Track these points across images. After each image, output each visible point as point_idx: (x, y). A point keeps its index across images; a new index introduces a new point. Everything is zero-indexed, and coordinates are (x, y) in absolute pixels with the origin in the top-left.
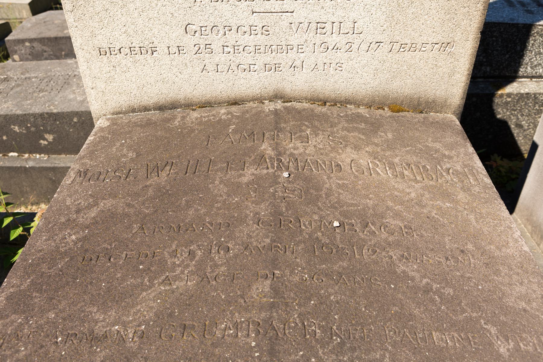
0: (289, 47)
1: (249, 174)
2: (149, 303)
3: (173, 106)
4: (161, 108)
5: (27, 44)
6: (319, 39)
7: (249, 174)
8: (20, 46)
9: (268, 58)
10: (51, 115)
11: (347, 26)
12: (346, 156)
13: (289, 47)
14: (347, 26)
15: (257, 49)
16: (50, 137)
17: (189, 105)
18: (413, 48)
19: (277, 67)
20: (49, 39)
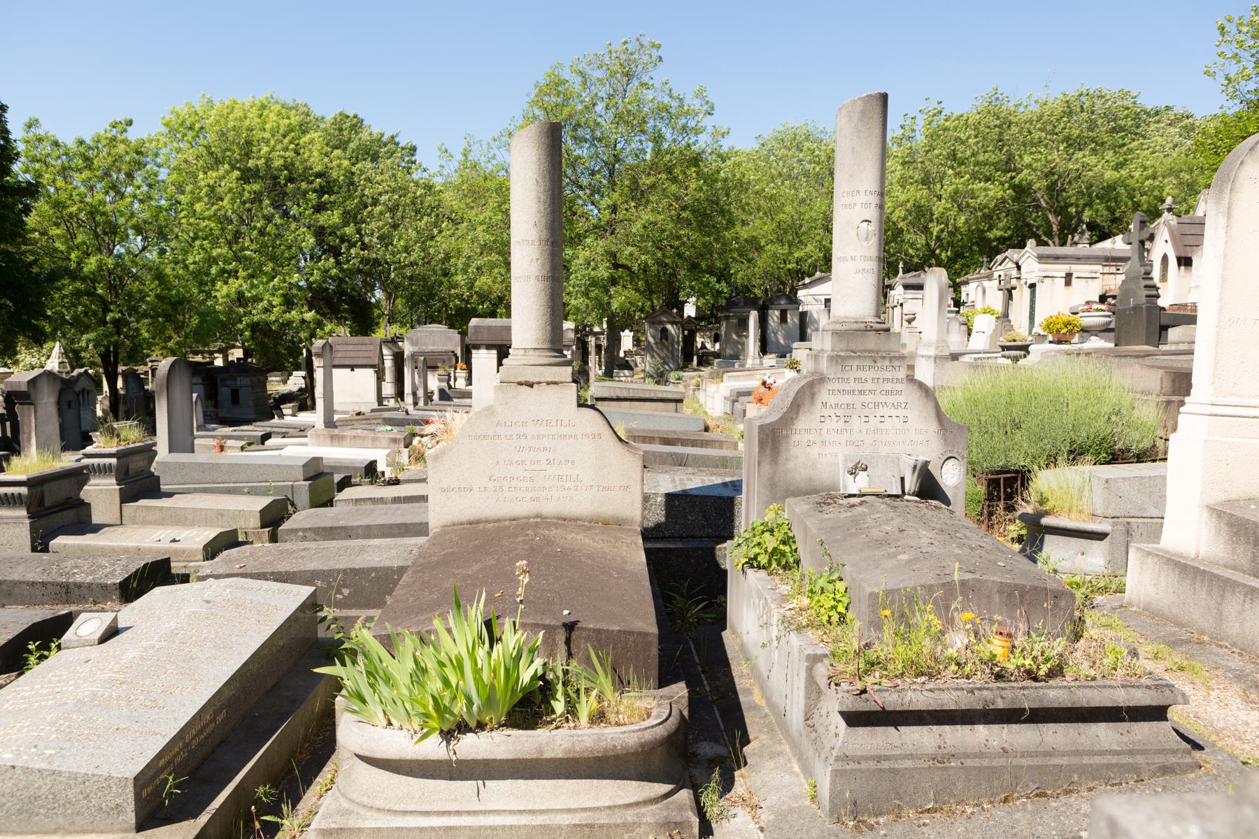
0: (544, 488)
1: (520, 539)
2: (476, 567)
3: (478, 522)
4: (470, 523)
5: (300, 534)
6: (560, 484)
7: (520, 539)
8: (292, 536)
9: (533, 494)
10: (352, 570)
11: (574, 477)
12: (569, 537)
13: (544, 488)
14: (574, 477)
15: (527, 489)
16: (346, 592)
17: (487, 521)
18: (609, 489)
19: (538, 499)
20: (324, 529)
